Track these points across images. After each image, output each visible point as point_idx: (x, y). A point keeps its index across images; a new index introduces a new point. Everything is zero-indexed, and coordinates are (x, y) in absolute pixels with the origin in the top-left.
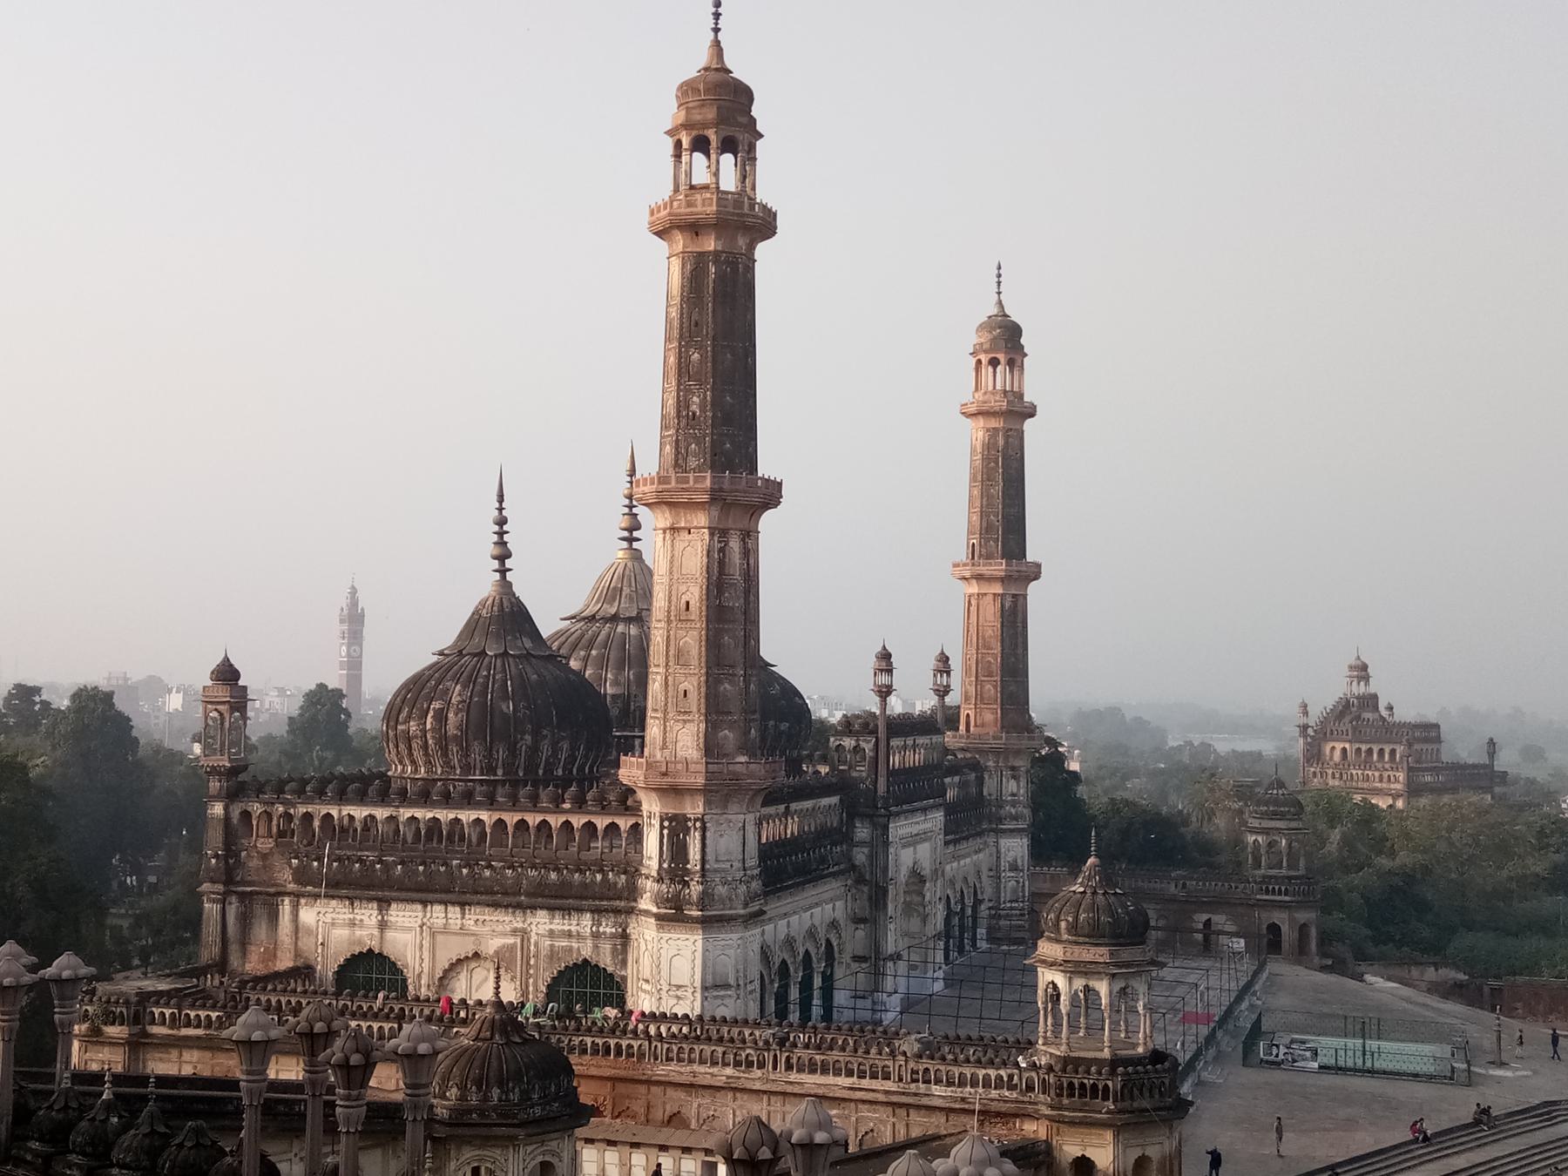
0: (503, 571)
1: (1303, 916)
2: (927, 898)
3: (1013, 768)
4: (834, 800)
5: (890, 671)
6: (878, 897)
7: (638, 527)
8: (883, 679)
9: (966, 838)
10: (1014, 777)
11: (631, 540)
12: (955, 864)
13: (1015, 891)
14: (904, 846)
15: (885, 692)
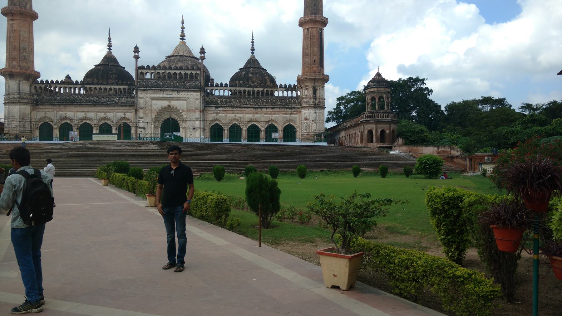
0: (110, 49)
1: (369, 127)
2: (185, 116)
3: (306, 86)
4: (122, 87)
5: (138, 52)
6: (136, 111)
7: (185, 36)
8: (137, 54)
9: (273, 108)
10: (306, 89)
11: (183, 39)
12: (256, 115)
13: (306, 126)
14: (153, 99)
15: (137, 58)
